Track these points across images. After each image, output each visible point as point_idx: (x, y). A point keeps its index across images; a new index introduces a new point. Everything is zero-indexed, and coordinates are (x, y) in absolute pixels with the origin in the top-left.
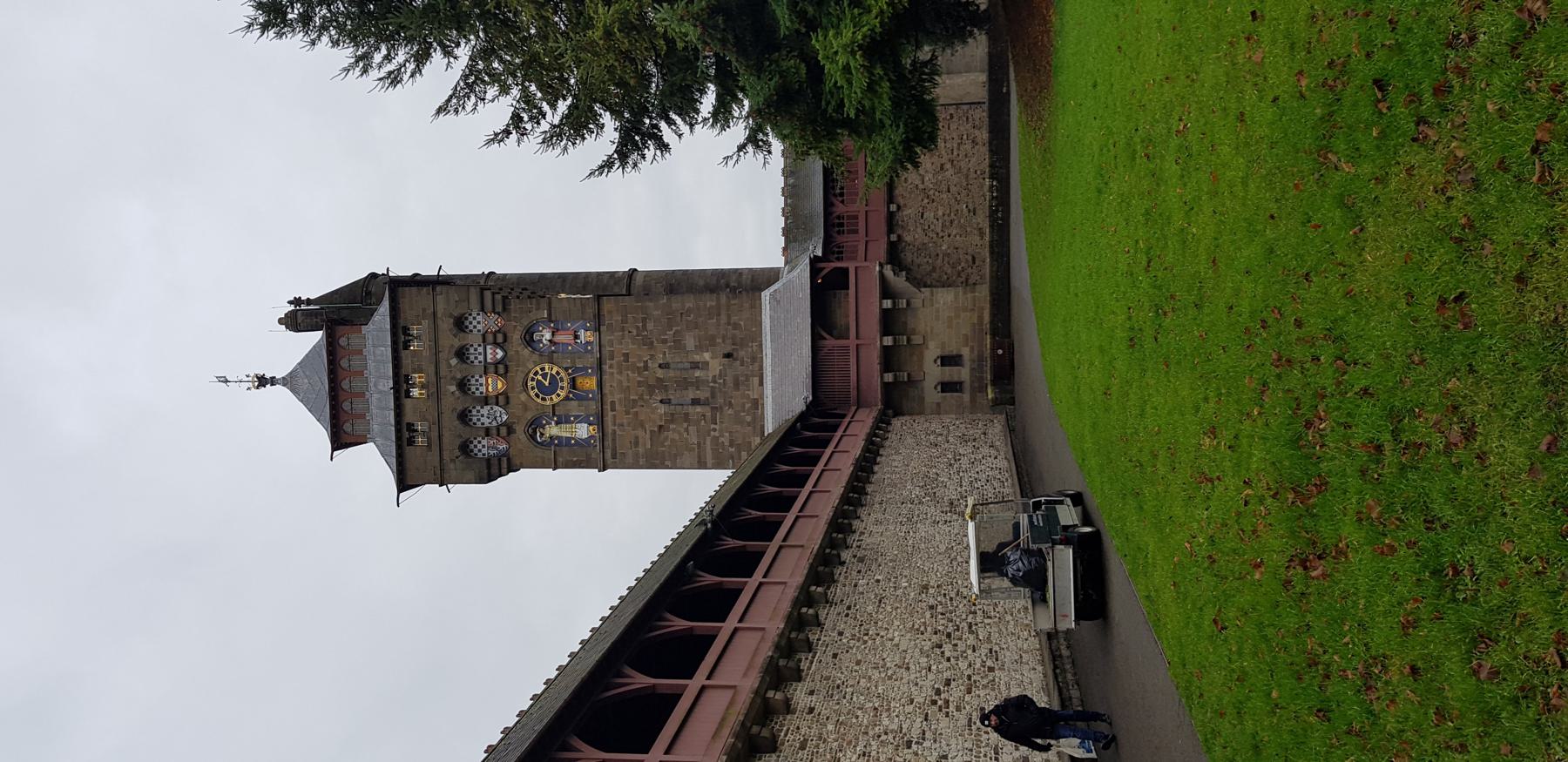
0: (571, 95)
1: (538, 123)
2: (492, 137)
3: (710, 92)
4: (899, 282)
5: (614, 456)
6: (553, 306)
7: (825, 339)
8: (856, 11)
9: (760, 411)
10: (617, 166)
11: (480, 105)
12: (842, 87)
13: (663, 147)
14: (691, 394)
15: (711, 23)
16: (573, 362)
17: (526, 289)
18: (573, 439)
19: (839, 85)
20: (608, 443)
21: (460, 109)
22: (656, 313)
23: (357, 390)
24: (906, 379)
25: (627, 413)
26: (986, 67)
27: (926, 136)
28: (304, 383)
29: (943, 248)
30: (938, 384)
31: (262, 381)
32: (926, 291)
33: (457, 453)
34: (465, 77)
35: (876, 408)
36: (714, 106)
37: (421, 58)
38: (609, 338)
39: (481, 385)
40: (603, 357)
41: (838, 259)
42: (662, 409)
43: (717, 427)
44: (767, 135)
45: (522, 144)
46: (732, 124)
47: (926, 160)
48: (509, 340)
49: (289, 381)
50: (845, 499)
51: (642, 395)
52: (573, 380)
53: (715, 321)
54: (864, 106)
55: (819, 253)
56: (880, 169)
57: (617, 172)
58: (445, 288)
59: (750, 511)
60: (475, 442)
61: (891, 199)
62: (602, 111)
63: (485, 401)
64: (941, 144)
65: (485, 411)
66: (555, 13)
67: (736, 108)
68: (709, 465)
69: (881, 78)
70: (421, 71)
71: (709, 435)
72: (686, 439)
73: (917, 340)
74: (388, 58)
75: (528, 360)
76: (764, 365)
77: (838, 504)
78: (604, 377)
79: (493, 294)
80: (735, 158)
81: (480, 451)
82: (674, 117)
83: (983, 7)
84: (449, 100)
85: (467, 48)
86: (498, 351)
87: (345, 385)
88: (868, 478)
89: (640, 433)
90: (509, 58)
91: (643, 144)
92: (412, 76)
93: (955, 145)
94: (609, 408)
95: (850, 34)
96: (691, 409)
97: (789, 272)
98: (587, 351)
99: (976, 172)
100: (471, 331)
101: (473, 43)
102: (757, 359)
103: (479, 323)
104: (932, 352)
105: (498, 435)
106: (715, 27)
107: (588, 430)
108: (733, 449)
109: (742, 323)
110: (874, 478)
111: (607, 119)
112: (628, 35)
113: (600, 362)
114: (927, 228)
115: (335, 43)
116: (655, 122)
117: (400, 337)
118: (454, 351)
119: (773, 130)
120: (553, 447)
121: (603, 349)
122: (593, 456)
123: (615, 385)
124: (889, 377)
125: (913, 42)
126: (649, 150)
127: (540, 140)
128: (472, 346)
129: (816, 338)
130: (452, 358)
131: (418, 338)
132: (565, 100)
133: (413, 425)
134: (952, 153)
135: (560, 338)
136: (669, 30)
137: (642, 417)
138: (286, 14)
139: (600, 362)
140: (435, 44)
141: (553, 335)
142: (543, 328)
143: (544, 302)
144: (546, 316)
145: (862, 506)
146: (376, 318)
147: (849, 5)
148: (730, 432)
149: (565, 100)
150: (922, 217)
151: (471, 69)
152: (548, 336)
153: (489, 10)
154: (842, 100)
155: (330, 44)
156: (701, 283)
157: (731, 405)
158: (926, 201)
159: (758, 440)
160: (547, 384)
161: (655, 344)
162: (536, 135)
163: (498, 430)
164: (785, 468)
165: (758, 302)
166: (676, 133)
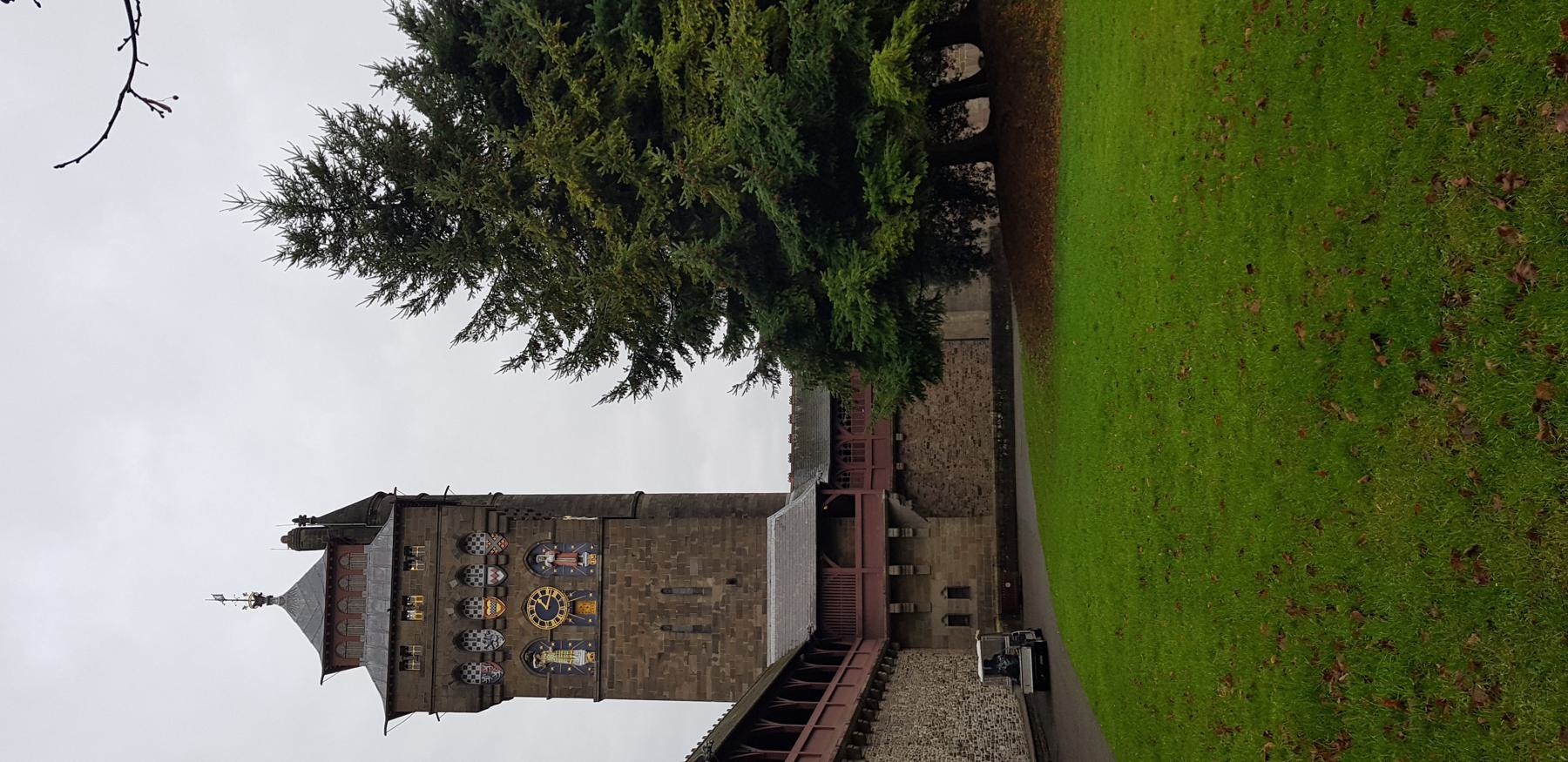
0: (588, 324)
1: (555, 350)
2: (509, 363)
3: (722, 324)
4: (905, 510)
5: (611, 686)
6: (557, 528)
7: (830, 566)
8: (864, 252)
9: (762, 641)
10: (629, 392)
11: (499, 332)
12: (851, 322)
13: (675, 374)
14: (693, 621)
15: (725, 260)
16: (575, 585)
17: (531, 511)
18: (570, 666)
19: (847, 320)
20: (606, 671)
21: (479, 336)
23: (355, 611)
24: (912, 611)
26: (989, 305)
27: (932, 370)
28: (301, 603)
29: (950, 478)
30: (946, 616)
31: (259, 600)
32: (933, 520)
34: (486, 306)
35: (882, 640)
36: (725, 337)
37: (445, 288)
39: (480, 608)
41: (845, 486)
42: (662, 636)
43: (718, 656)
44: (776, 365)
45: (538, 370)
46: (742, 355)
47: (931, 392)
49: (286, 601)
50: (850, 738)
51: (643, 621)
52: (574, 604)
53: (719, 545)
54: (870, 340)
55: (826, 480)
56: (887, 400)
57: (628, 398)
58: (450, 508)
59: (749, 748)
60: (470, 668)
61: (897, 429)
62: (617, 341)
63: (483, 624)
64: (946, 377)
65: (481, 635)
66: (577, 249)
67: (747, 340)
68: (708, 697)
69: (888, 315)
70: (444, 300)
71: (710, 665)
73: (923, 570)
74: (413, 287)
76: (768, 592)
77: (843, 741)
78: (607, 602)
79: (499, 515)
80: (745, 386)
81: (473, 677)
82: (687, 346)
83: (985, 251)
84: (469, 328)
85: (490, 279)
86: (500, 573)
87: (342, 605)
88: (874, 715)
89: (639, 661)
90: (530, 289)
91: (655, 371)
92: (435, 304)
93: (960, 379)
94: (608, 633)
95: (858, 274)
97: (795, 498)
98: (589, 575)
99: (981, 405)
100: (474, 552)
101: (496, 274)
102: (761, 586)
103: (482, 544)
104: (939, 583)
105: (493, 661)
106: (730, 264)
108: (734, 681)
109: (747, 548)
110: (880, 715)
111: (622, 347)
112: (645, 271)
113: (602, 586)
114: (933, 457)
115: (363, 272)
116: (668, 351)
117: (402, 556)
118: (454, 575)
119: (782, 361)
120: (548, 674)
121: (605, 572)
122: (589, 685)
123: (616, 609)
124: (895, 608)
125: (918, 280)
126: (661, 377)
127: (555, 366)
128: (473, 567)
129: (821, 565)
130: (452, 580)
131: (420, 558)
132: (581, 329)
133: (407, 648)
134: (957, 386)
135: (564, 560)
136: (685, 266)
137: (641, 645)
138: (318, 244)
139: (602, 586)
140: (459, 275)
141: (556, 557)
142: (547, 551)
143: (549, 524)
145: (867, 745)
146: (380, 537)
147: (858, 247)
148: (732, 663)
149: (581, 329)
150: (928, 448)
151: (493, 298)
152: (550, 558)
153: (514, 245)
154: (850, 334)
155: (358, 273)
156: (707, 506)
157: (733, 634)
158: (932, 431)
159: (760, 671)
160: (546, 607)
161: (659, 568)
162: (552, 361)
163: (494, 654)
164: (788, 702)
165: (763, 527)
166: (688, 362)
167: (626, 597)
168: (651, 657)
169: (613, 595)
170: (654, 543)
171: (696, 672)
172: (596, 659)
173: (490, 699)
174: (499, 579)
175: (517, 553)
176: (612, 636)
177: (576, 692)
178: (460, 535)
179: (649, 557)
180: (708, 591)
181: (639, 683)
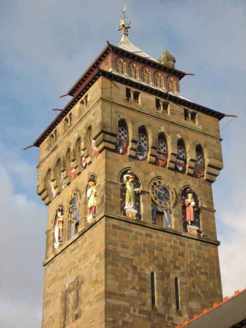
5: (114, 227)
22: (211, 284)
25: (145, 245)
42: (148, 272)
68: (108, 300)
72: (128, 287)
94: (148, 232)
96: (149, 295)
121: (186, 239)
122: (114, 211)
137: (142, 255)
148: (133, 324)
171: (125, 293)
173: (108, 139)
174: (178, 166)
175: (192, 182)
176: (147, 235)
177: (109, 200)
180: (179, 314)
181: (116, 247)
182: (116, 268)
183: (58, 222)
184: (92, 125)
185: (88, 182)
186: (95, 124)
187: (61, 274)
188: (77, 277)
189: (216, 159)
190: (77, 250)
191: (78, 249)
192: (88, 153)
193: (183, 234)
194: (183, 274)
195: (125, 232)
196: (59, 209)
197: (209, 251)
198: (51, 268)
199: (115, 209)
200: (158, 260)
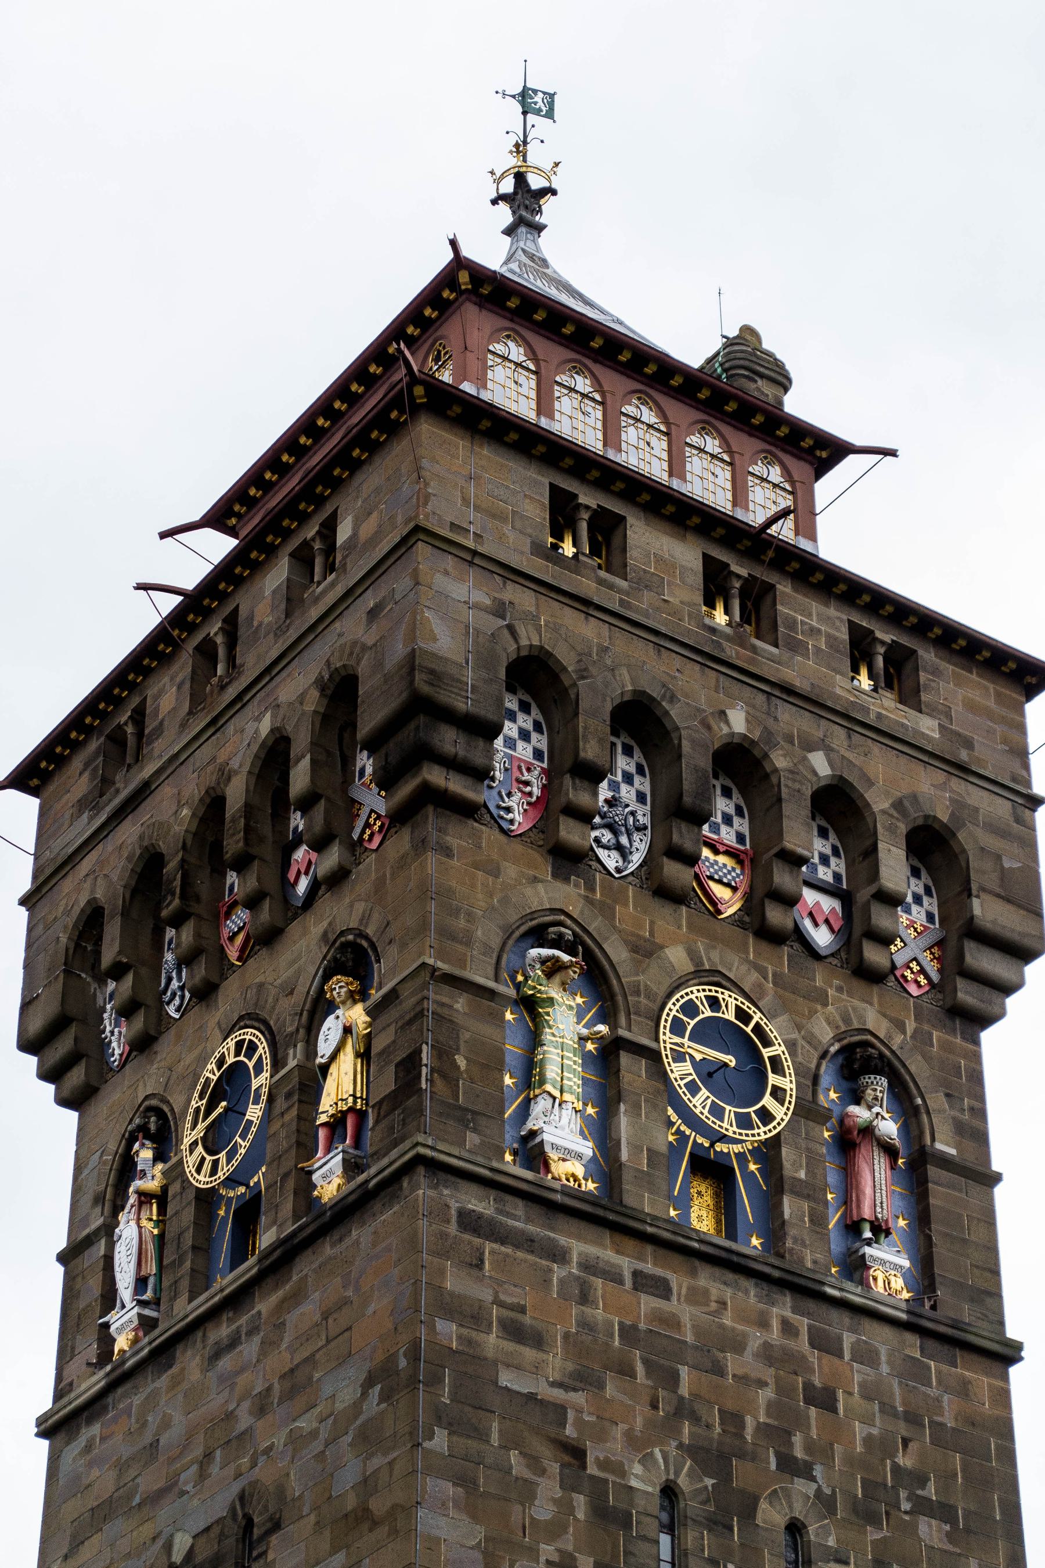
5: (469, 1222)
25: (628, 1333)
33: (529, 637)
38: (883, 1358)
40: (823, 1309)
48: (858, 985)
51: (695, 1419)
60: (525, 721)
75: (799, 1027)
78: (750, 1295)
94: (649, 1267)
107: (568, 1155)
121: (846, 1318)
122: (472, 1139)
123: (727, 1322)
141: (890, 1151)
144: (945, 1147)
152: (889, 1128)
161: (873, 1534)
167: (768, 1374)
168: (571, 1415)
169: (775, 1324)
170: (948, 1535)
172: (566, 1191)
175: (884, 1015)
177: (444, 1076)
178: (961, 836)
179: (906, 1506)
182: (473, 1444)
183: (133, 1199)
184: (363, 669)
185: (326, 977)
186: (379, 664)
187: (149, 1481)
188: (242, 1497)
189: (1008, 900)
190: (250, 1349)
191: (257, 1340)
192: (327, 822)
193: (830, 1291)
194: (826, 1503)
195: (530, 1257)
196: (143, 1129)
197: (963, 1390)
198: (88, 1448)
199: (475, 1130)
200: (695, 1419)
